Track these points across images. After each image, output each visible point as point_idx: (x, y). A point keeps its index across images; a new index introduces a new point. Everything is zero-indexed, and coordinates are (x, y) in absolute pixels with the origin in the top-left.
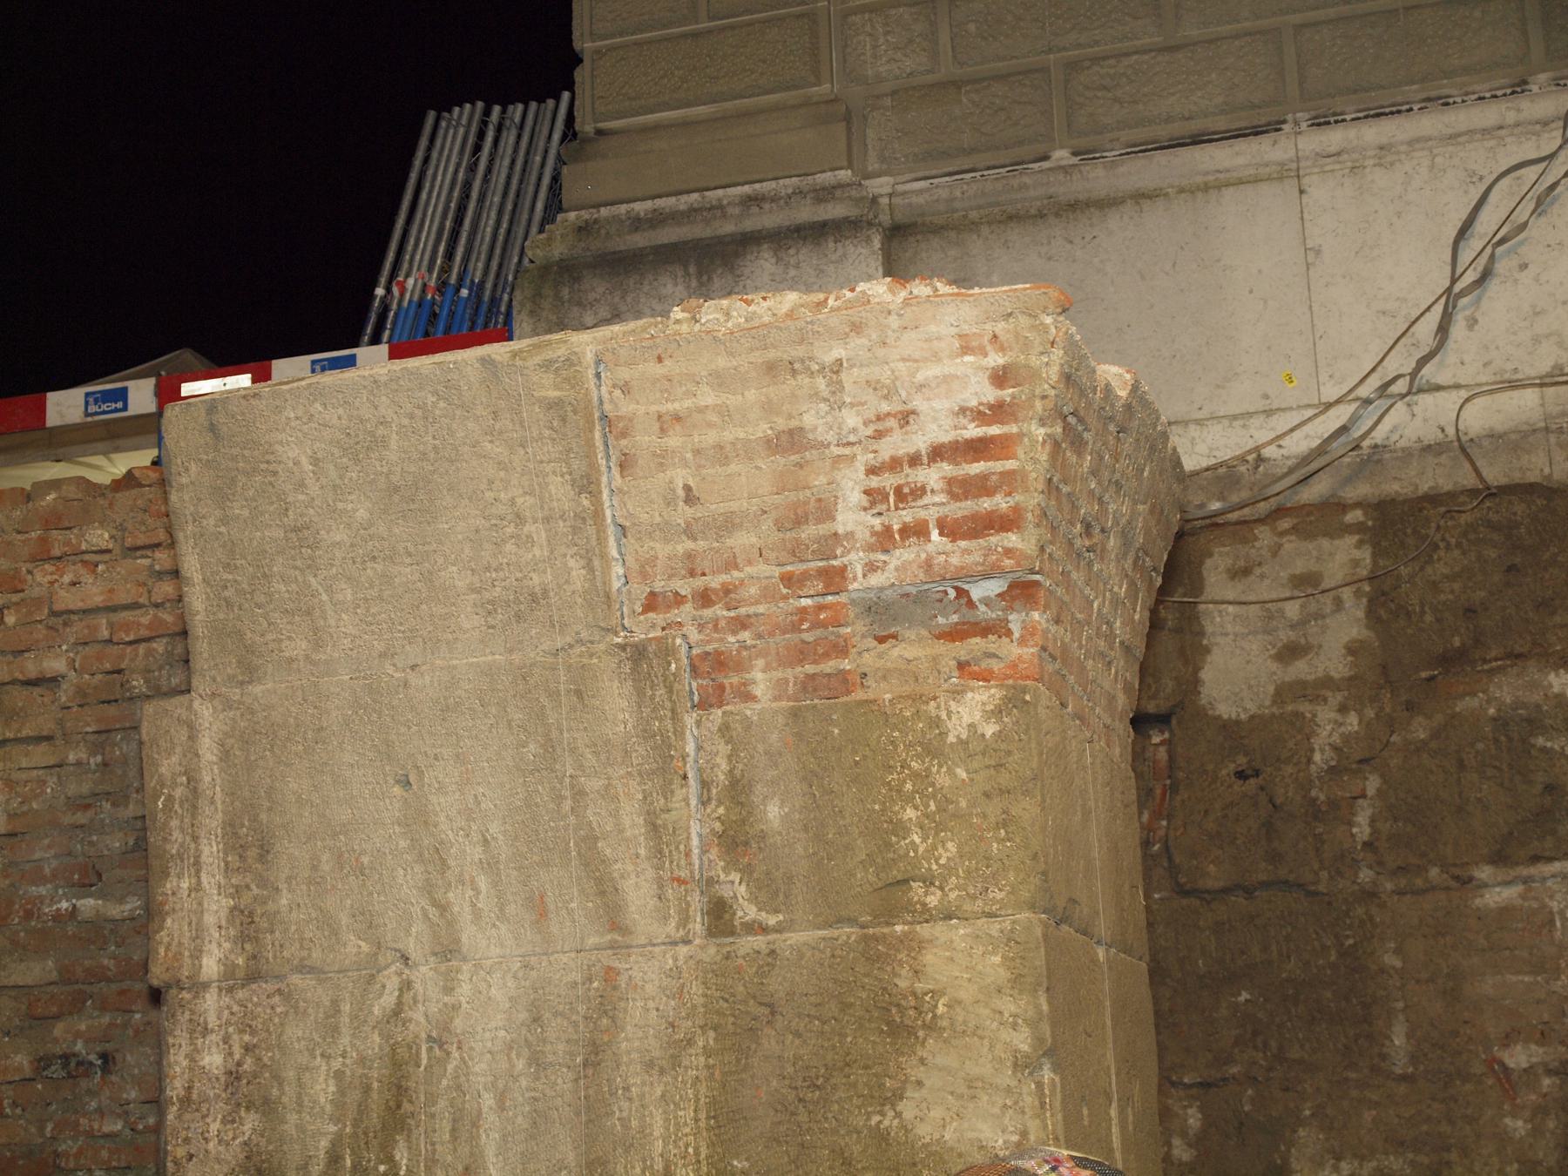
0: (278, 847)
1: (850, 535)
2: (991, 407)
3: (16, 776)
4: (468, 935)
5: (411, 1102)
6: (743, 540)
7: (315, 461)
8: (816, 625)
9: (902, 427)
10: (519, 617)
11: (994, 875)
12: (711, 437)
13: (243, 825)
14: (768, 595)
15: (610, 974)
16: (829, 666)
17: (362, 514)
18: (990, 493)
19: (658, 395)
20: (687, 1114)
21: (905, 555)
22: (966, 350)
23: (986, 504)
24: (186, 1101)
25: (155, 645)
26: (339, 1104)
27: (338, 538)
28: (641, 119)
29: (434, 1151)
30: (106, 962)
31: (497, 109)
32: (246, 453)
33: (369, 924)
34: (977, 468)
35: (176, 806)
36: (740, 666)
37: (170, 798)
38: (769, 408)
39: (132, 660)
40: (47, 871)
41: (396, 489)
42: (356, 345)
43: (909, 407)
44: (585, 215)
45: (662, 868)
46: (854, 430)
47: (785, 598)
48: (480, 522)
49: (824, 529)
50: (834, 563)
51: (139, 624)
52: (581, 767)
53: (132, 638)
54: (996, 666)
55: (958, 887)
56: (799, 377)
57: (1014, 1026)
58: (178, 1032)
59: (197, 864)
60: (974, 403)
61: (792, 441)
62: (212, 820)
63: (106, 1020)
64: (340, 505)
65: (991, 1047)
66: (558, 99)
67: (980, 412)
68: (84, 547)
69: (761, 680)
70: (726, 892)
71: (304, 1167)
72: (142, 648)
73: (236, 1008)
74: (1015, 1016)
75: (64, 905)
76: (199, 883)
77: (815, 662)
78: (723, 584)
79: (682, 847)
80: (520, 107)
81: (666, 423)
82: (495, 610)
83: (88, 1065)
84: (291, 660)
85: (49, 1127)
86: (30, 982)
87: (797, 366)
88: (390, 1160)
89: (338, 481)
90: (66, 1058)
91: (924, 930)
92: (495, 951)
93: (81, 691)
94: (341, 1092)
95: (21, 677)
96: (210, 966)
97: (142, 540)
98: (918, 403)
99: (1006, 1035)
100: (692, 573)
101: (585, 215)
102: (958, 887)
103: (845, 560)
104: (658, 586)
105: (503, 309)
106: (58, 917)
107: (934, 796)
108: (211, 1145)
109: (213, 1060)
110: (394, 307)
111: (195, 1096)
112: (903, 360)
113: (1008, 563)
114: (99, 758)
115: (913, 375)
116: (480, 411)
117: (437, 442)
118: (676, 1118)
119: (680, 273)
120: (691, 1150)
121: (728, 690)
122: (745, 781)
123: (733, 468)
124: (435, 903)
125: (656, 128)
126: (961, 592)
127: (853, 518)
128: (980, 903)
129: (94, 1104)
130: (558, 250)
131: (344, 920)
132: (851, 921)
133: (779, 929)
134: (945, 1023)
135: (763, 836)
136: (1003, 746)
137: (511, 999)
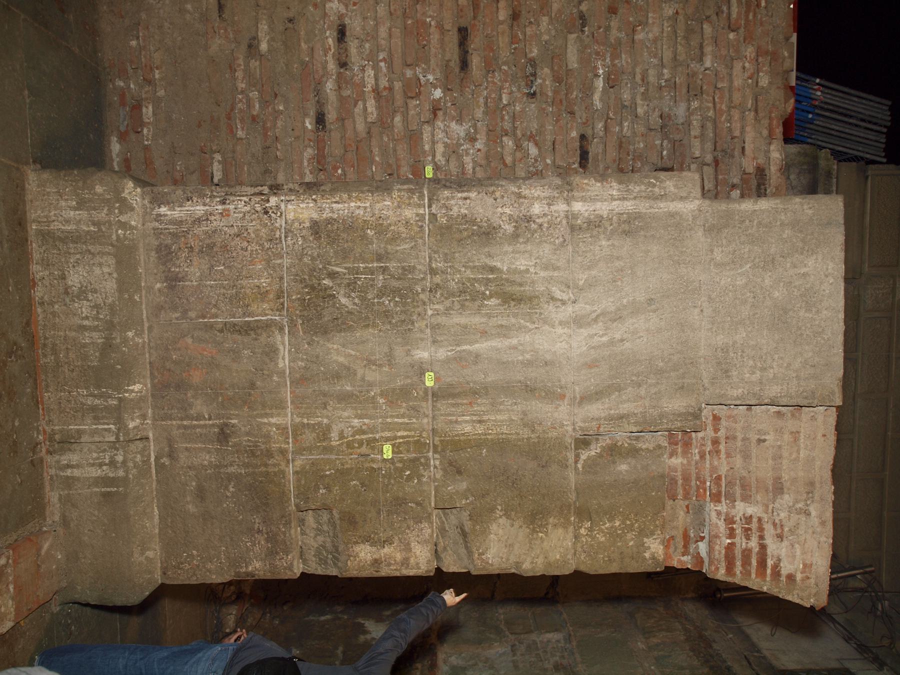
0: (628, 239)
1: (734, 507)
2: (779, 571)
3: (659, 43)
4: (584, 332)
5: (515, 306)
6: (738, 461)
7: (805, 275)
8: (698, 488)
9: (777, 535)
10: (719, 363)
11: (591, 555)
12: (785, 454)
13: (639, 222)
14: (714, 469)
15: (563, 397)
16: (680, 491)
17: (777, 294)
18: (743, 565)
19: (808, 432)
20: (505, 430)
21: (722, 526)
22: (805, 565)
23: (738, 563)
24: (519, 196)
25: (711, 112)
26: (516, 271)
27: (766, 281)
28: (869, 195)
29: (494, 317)
30: (575, 93)
31: (885, 130)
32: (814, 241)
33: (591, 284)
34: (754, 562)
35: (650, 189)
36: (685, 453)
37: (654, 185)
38: (794, 480)
39: (706, 100)
40: (617, 61)
41: (786, 313)
42: (797, 70)
43: (785, 539)
44: (834, 173)
45: (605, 420)
46: (778, 515)
47: (711, 476)
48: (765, 351)
49: (738, 495)
50: (723, 499)
51: (722, 104)
52: (650, 386)
53: (717, 100)
54: (671, 550)
55: (587, 541)
56: (805, 495)
57: (532, 563)
58: (550, 191)
59: (624, 199)
60: (782, 565)
61: (778, 489)
62: (643, 207)
63: (550, 94)
64: (782, 284)
65: (525, 554)
66: (884, 157)
67: (777, 566)
68: (761, 74)
69: (677, 461)
70: (593, 446)
71: (490, 255)
72: (711, 105)
73: (559, 219)
74: (536, 563)
75: (601, 71)
76: (615, 200)
77: (682, 484)
78: (720, 450)
79: (613, 429)
80: (884, 141)
81: (796, 435)
82: (723, 353)
83: (530, 85)
84: (712, 251)
85: (505, 68)
86: (569, 55)
87: (811, 495)
88: (491, 296)
89: (793, 285)
90: (534, 75)
91: (571, 529)
92: (575, 345)
93: (694, 74)
94: (520, 272)
95: (704, 44)
96: (578, 206)
97: (760, 104)
98: (785, 543)
99: (529, 560)
100: (727, 438)
101: (834, 173)
102: (587, 541)
103: (724, 503)
104: (723, 422)
105: (801, 133)
106: (596, 68)
107: (623, 532)
108: (500, 209)
109: (537, 209)
110: (810, 86)
111: (521, 200)
112: (805, 539)
113: (713, 568)
114: (663, 84)
115: (798, 543)
116: (817, 359)
117: (805, 336)
118: (504, 425)
120: (490, 431)
121: (675, 447)
122: (637, 455)
123: (770, 462)
124: (598, 316)
125: (864, 201)
126: (702, 538)
127: (742, 509)
128: (580, 550)
129: (514, 89)
130: (822, 163)
131: (594, 273)
132: (577, 497)
133: (576, 468)
134: (535, 536)
135: (614, 462)
136: (640, 560)
137: (555, 352)
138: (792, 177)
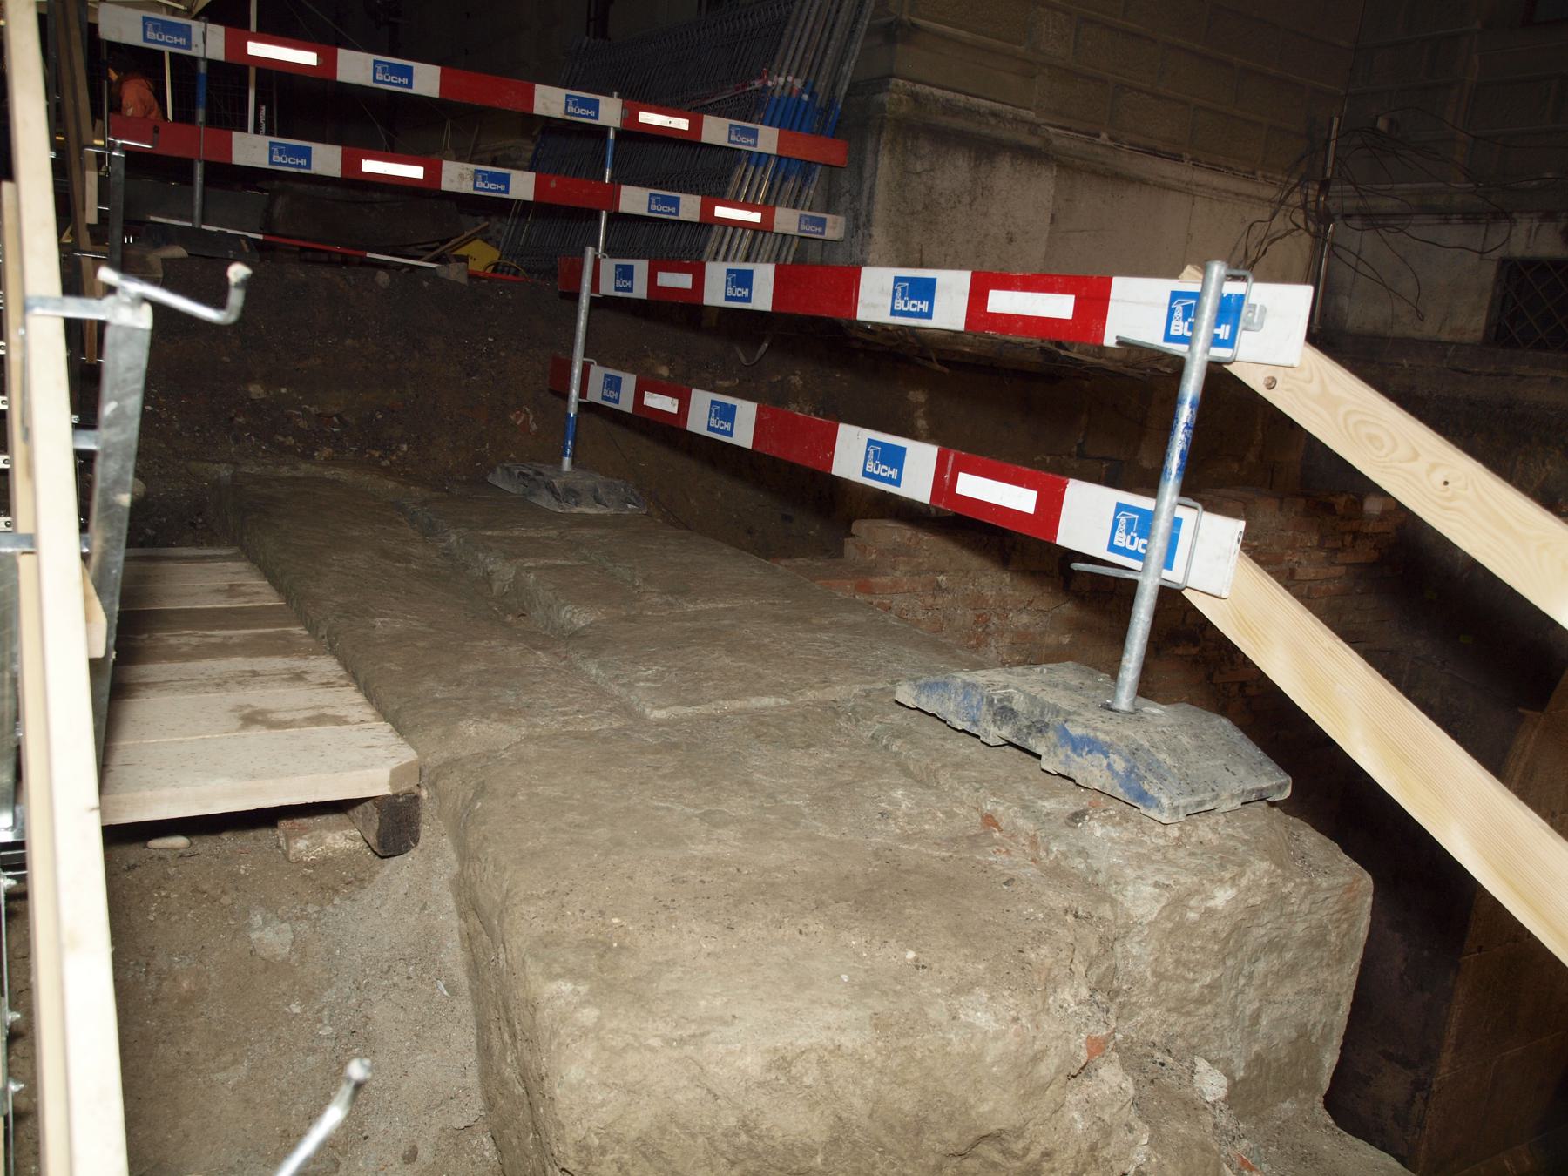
101: (909, 85)
119: (967, 155)
138: (919, 168)
